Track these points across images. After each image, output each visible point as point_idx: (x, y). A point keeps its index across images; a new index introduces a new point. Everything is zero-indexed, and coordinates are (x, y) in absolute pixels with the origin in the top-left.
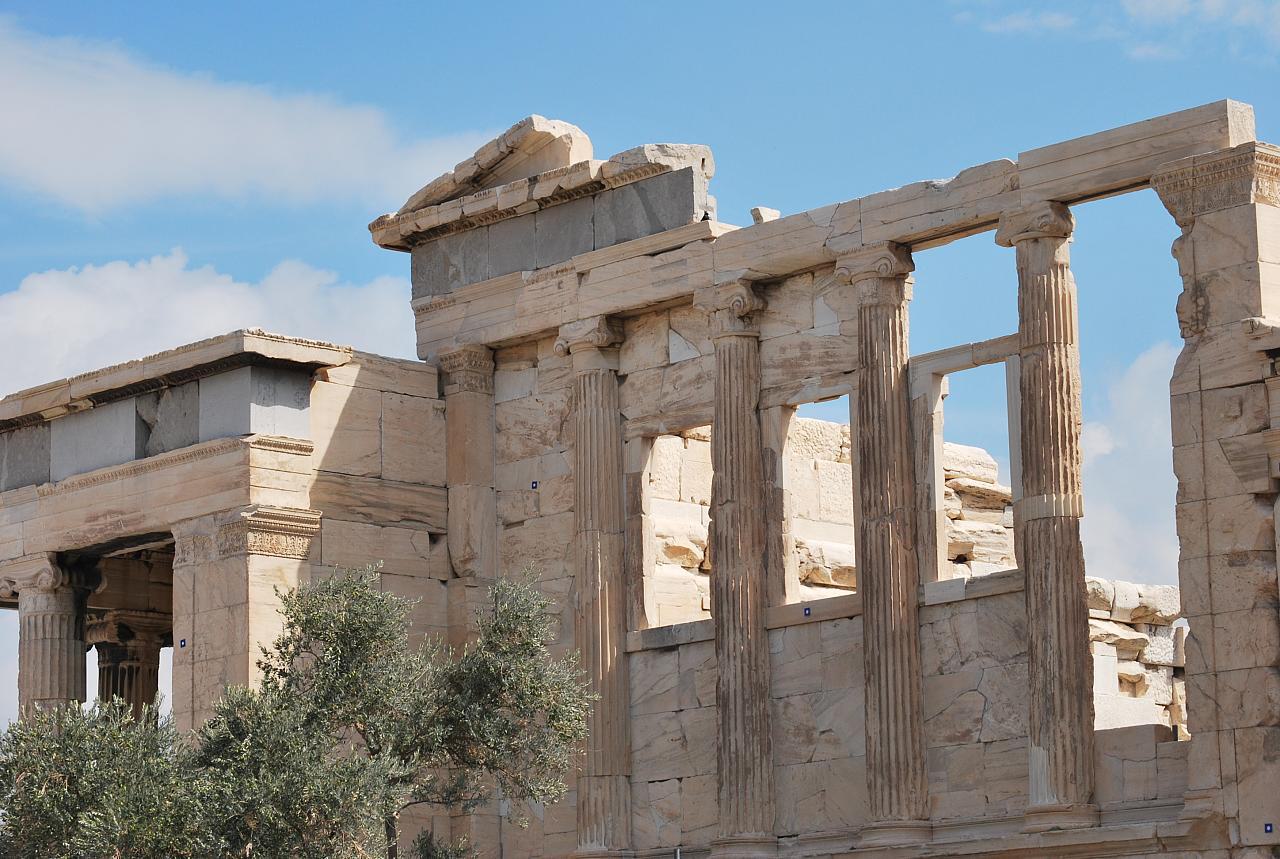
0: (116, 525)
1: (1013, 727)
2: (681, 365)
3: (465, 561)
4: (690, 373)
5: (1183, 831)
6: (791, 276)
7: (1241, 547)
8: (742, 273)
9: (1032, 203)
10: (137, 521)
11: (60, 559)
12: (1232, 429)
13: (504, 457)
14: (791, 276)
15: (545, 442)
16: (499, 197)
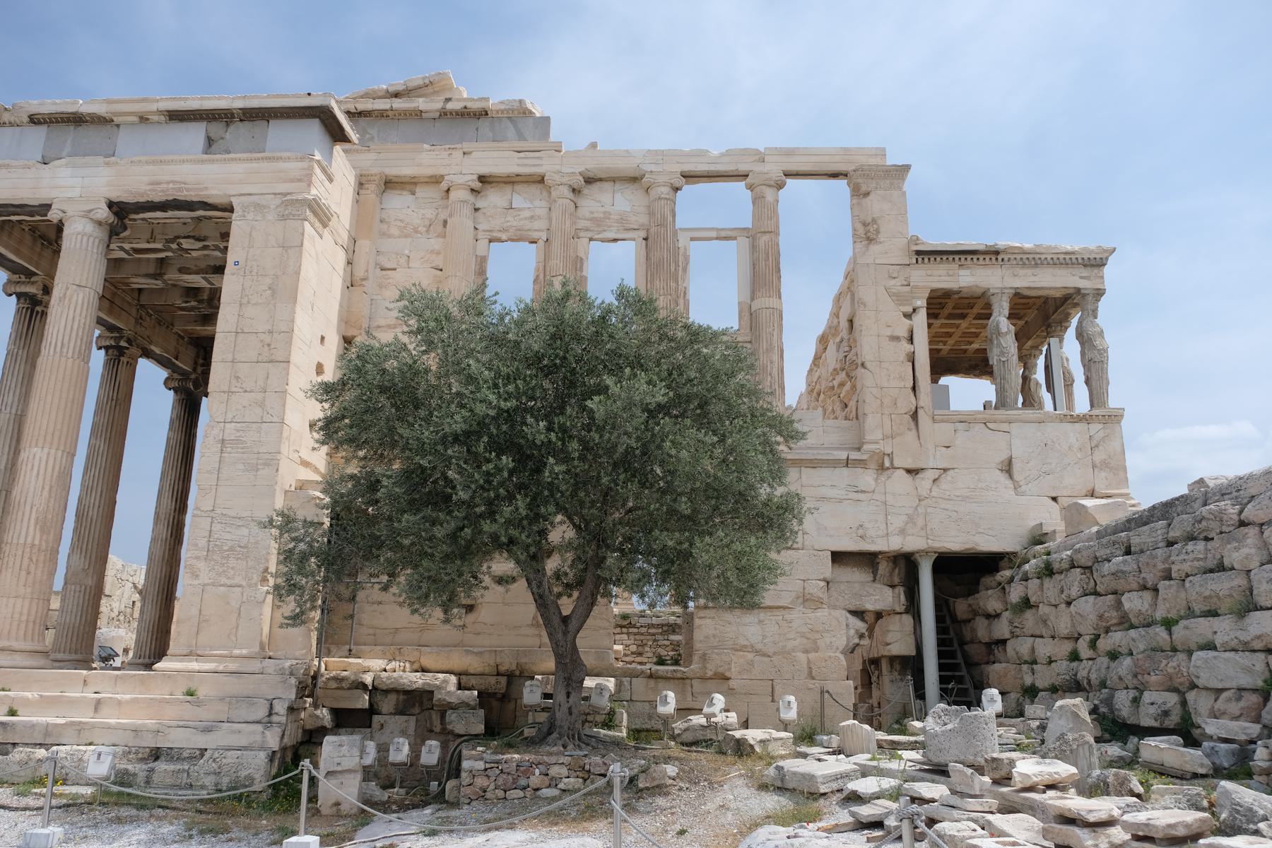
0: (179, 190)
2: (520, 210)
3: (364, 279)
4: (527, 214)
5: (865, 457)
6: (601, 180)
8: (582, 169)
9: (774, 169)
10: (201, 190)
11: (111, 205)
12: (893, 282)
13: (383, 234)
14: (601, 180)
15: (417, 232)
16: (420, 103)
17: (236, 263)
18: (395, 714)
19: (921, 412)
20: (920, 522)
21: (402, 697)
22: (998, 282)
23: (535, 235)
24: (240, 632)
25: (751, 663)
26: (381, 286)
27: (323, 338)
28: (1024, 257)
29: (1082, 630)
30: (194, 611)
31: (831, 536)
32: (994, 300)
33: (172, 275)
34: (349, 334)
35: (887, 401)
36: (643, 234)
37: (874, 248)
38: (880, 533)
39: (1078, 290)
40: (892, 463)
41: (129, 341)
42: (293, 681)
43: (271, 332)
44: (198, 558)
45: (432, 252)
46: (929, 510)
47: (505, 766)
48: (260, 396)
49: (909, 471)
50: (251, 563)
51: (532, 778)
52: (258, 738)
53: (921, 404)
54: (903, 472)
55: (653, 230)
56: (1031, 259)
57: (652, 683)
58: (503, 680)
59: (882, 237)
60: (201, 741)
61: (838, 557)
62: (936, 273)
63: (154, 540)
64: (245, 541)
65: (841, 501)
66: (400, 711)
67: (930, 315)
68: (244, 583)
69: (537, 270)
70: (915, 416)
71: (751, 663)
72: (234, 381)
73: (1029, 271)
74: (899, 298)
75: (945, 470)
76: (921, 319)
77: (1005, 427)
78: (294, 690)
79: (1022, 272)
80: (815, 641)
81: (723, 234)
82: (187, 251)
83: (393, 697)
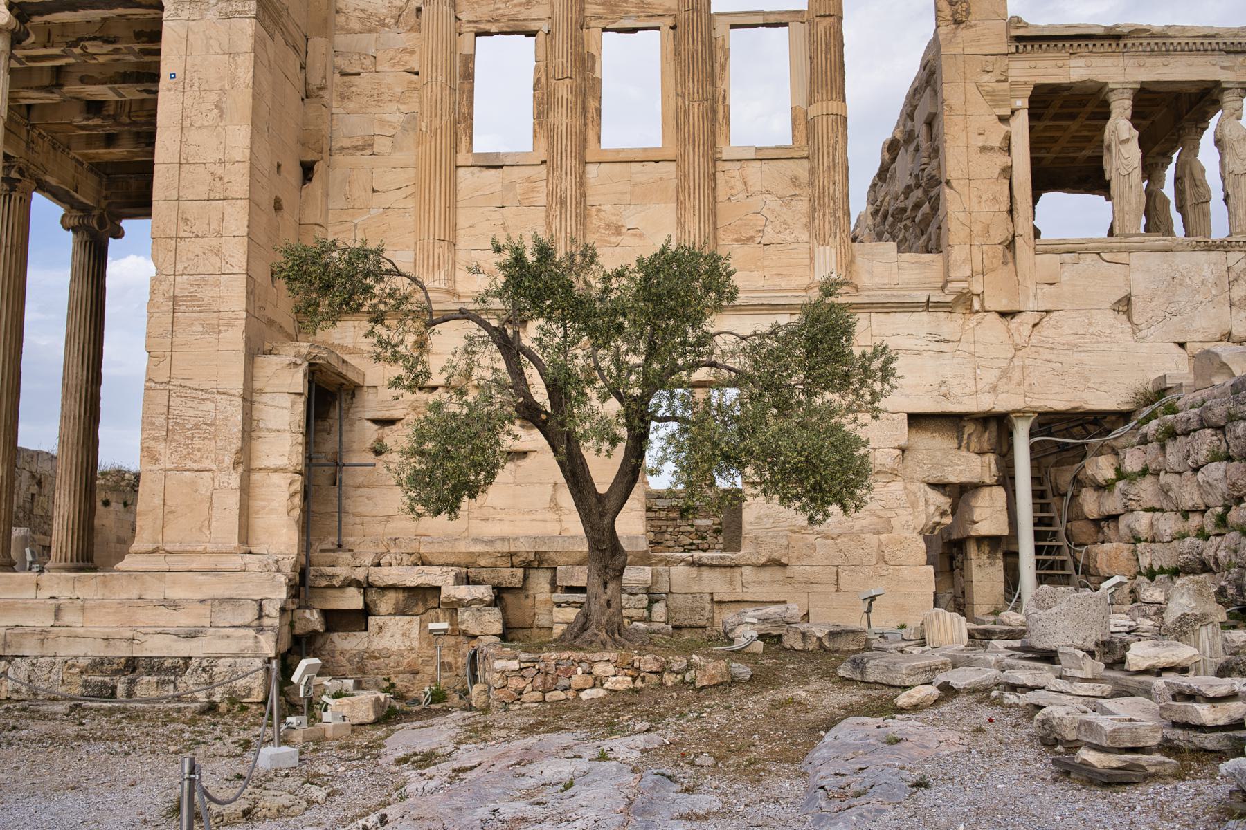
1: (786, 236)
3: (320, 89)
5: (950, 298)
7: (989, 144)
12: (986, 77)
15: (383, 25)
17: (173, 76)
18: (395, 614)
19: (1019, 241)
20: (1017, 376)
21: (401, 595)
22: (1120, 73)
23: (533, 26)
24: (214, 524)
25: (813, 547)
26: (343, 97)
27: (279, 166)
28: (1153, 41)
29: (1211, 500)
30: (158, 501)
31: (907, 396)
32: (1112, 97)
33: (73, 88)
34: (308, 158)
35: (977, 229)
36: (669, 21)
37: (962, 33)
38: (967, 390)
39: (1217, 83)
40: (982, 305)
41: (21, 172)
42: (282, 579)
43: (221, 162)
44: (156, 439)
45: (404, 51)
46: (1027, 362)
47: (542, 665)
48: (214, 242)
49: (1003, 314)
50: (220, 444)
51: (574, 678)
52: (250, 643)
53: (1019, 231)
54: (997, 316)
55: (681, 18)
56: (1161, 42)
57: (694, 571)
58: (519, 572)
59: (972, 19)
60: (183, 648)
61: (916, 420)
62: (1041, 64)
63: (64, 418)
64: (211, 417)
65: (919, 353)
66: (401, 612)
67: (1032, 116)
68: (214, 467)
69: (537, 71)
70: (1010, 245)
71: (813, 547)
72: (181, 224)
73: (1159, 60)
74: (992, 98)
75: (1047, 312)
76: (1021, 124)
77: (1123, 257)
78: (285, 589)
79: (1150, 61)
80: (888, 520)
81: (771, 20)
82: (93, 56)
83: (392, 597)
